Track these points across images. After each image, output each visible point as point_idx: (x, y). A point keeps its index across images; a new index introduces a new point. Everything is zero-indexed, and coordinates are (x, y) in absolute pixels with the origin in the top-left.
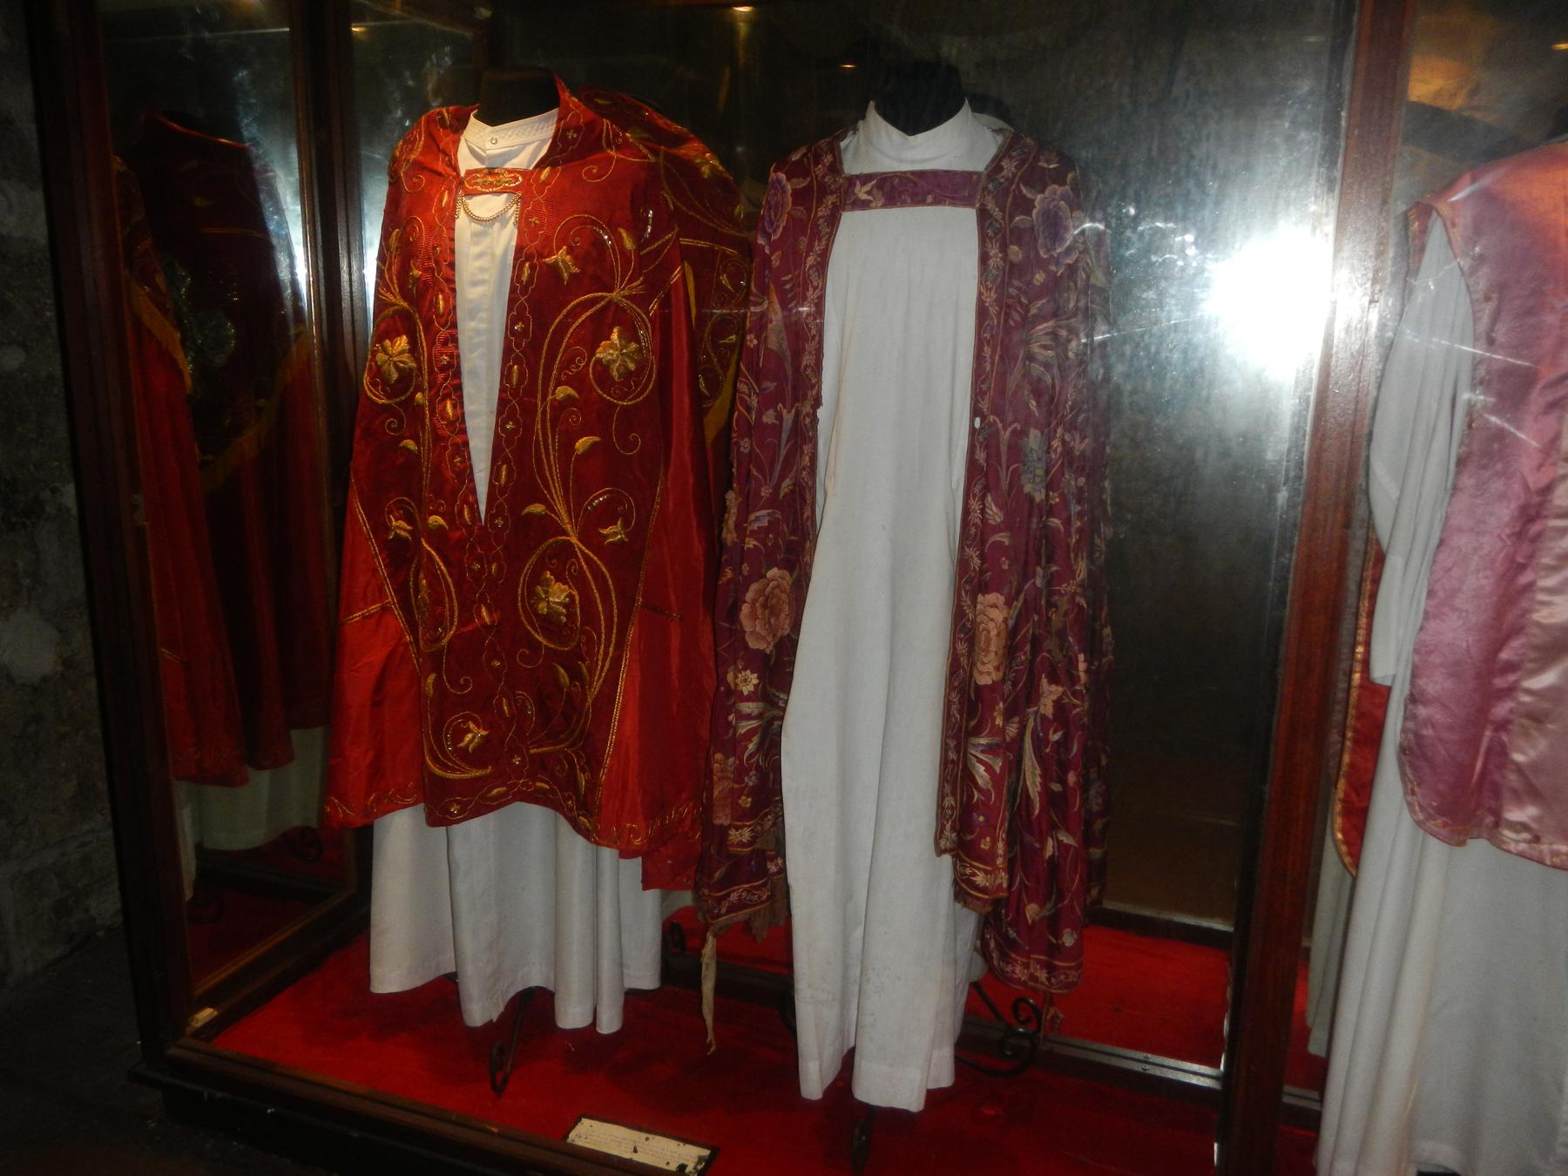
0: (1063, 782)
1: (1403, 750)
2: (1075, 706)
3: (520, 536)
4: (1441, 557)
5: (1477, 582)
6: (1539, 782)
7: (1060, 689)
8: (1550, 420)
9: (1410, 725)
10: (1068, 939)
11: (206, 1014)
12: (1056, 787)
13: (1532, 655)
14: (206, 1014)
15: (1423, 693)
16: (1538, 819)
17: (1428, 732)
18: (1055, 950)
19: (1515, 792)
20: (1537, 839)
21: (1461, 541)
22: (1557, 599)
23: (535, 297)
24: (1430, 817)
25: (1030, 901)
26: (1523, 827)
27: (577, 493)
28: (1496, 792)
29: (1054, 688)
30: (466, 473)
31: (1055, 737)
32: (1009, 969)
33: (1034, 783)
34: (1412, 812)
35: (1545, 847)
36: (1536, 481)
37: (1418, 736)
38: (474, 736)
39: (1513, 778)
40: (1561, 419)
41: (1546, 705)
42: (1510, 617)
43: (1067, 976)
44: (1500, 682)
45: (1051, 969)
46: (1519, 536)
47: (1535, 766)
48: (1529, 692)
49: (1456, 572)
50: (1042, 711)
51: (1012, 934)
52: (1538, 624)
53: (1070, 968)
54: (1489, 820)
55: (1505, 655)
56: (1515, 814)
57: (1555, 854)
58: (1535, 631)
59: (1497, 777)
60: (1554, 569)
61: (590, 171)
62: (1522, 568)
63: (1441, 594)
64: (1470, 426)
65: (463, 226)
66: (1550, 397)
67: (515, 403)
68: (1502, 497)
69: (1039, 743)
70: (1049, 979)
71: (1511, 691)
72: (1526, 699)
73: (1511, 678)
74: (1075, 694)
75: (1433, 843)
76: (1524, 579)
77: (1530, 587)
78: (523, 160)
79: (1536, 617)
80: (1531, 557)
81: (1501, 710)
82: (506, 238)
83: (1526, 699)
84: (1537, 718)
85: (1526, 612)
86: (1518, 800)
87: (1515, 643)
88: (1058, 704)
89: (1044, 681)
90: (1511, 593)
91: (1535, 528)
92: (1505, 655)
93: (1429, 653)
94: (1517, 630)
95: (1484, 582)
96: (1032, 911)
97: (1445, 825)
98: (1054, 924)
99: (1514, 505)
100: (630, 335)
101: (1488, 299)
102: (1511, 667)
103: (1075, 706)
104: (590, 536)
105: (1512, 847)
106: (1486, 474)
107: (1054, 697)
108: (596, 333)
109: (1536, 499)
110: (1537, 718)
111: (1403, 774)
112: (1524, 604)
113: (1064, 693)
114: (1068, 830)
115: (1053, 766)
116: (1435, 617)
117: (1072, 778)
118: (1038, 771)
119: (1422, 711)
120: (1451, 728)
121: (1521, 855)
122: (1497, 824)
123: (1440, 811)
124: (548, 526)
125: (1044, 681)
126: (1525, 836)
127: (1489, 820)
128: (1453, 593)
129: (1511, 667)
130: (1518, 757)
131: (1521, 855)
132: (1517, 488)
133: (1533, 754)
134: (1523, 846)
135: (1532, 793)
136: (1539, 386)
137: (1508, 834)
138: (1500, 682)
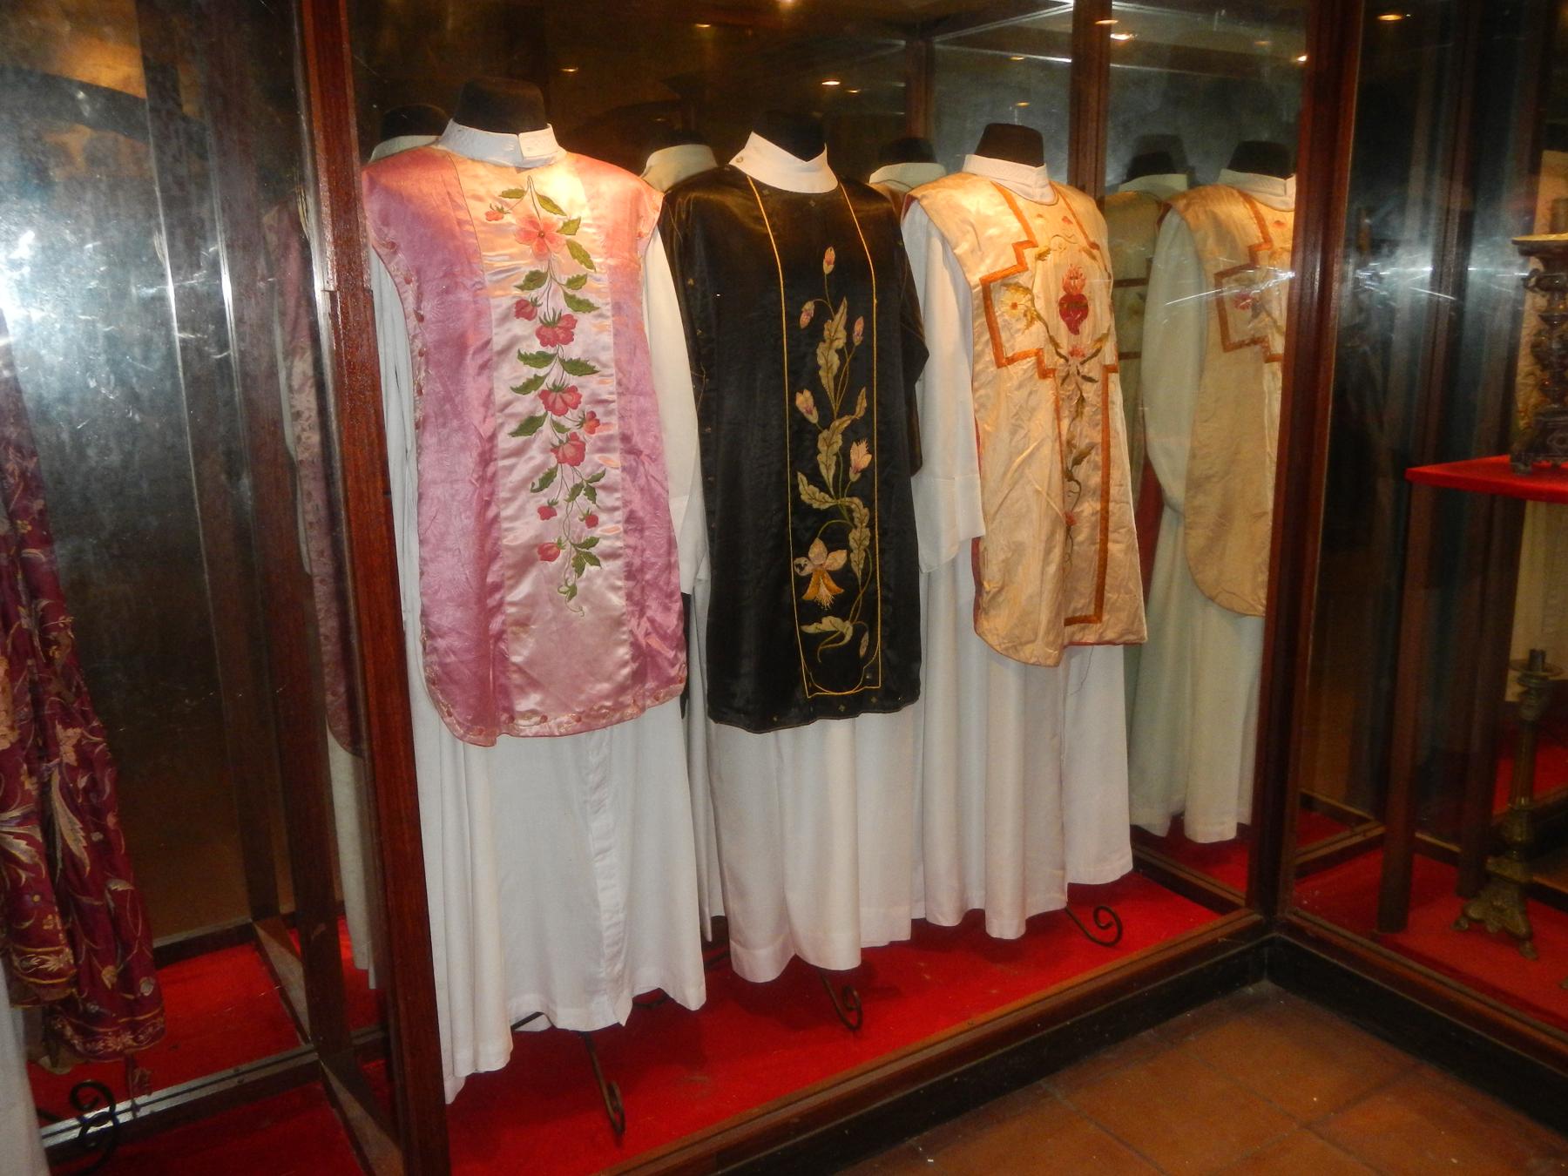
0: (102, 829)
1: (431, 681)
2: (96, 744)
4: (425, 508)
5: (463, 522)
6: (534, 674)
7: (78, 730)
8: (483, 379)
9: (434, 658)
10: (146, 989)
12: (97, 837)
13: (509, 573)
15: (438, 628)
16: (541, 703)
17: (451, 659)
18: (141, 1004)
19: (517, 686)
20: (544, 719)
21: (437, 492)
22: (517, 524)
24: (468, 730)
25: (104, 965)
26: (533, 712)
28: (505, 692)
29: (70, 732)
31: (82, 782)
32: (101, 1045)
33: (76, 840)
34: (452, 731)
35: (552, 723)
36: (486, 430)
37: (443, 665)
39: (516, 678)
40: (490, 378)
41: (527, 611)
42: (488, 547)
43: (154, 1025)
44: (491, 602)
45: (134, 1028)
46: (482, 479)
47: (531, 662)
48: (513, 604)
49: (441, 518)
50: (65, 760)
51: (93, 1008)
52: (508, 548)
53: (155, 1017)
54: (504, 717)
55: (490, 580)
56: (529, 702)
57: (559, 725)
58: (507, 553)
59: (502, 680)
60: (509, 501)
62: (488, 504)
63: (433, 540)
64: (420, 392)
66: (480, 361)
68: (463, 448)
69: (69, 795)
70: (135, 1040)
71: (501, 604)
72: (511, 610)
73: (497, 596)
74: (92, 732)
75: (474, 749)
76: (491, 513)
77: (496, 519)
79: (505, 542)
80: (492, 494)
81: (495, 625)
83: (511, 610)
84: (523, 623)
85: (498, 539)
86: (522, 691)
87: (496, 567)
88: (78, 748)
89: (59, 727)
90: (487, 527)
91: (490, 470)
92: (490, 580)
93: (436, 592)
94: (494, 556)
95: (466, 522)
96: (108, 975)
97: (481, 732)
98: (127, 980)
99: (475, 454)
101: (408, 282)
102: (497, 587)
103: (96, 744)
105: (528, 732)
106: (445, 432)
107: (74, 741)
109: (487, 447)
110: (523, 623)
111: (436, 703)
112: (495, 534)
113: (83, 736)
114: (119, 877)
115: (89, 815)
116: (432, 561)
117: (111, 820)
118: (78, 825)
119: (441, 643)
120: (468, 650)
121: (536, 736)
122: (512, 719)
123: (474, 722)
125: (59, 727)
126: (536, 719)
127: (504, 717)
128: (443, 536)
129: (497, 587)
130: (516, 659)
131: (536, 736)
132: (475, 440)
133: (526, 653)
134: (536, 729)
135: (534, 684)
136: (471, 351)
137: (521, 722)
138: (491, 602)
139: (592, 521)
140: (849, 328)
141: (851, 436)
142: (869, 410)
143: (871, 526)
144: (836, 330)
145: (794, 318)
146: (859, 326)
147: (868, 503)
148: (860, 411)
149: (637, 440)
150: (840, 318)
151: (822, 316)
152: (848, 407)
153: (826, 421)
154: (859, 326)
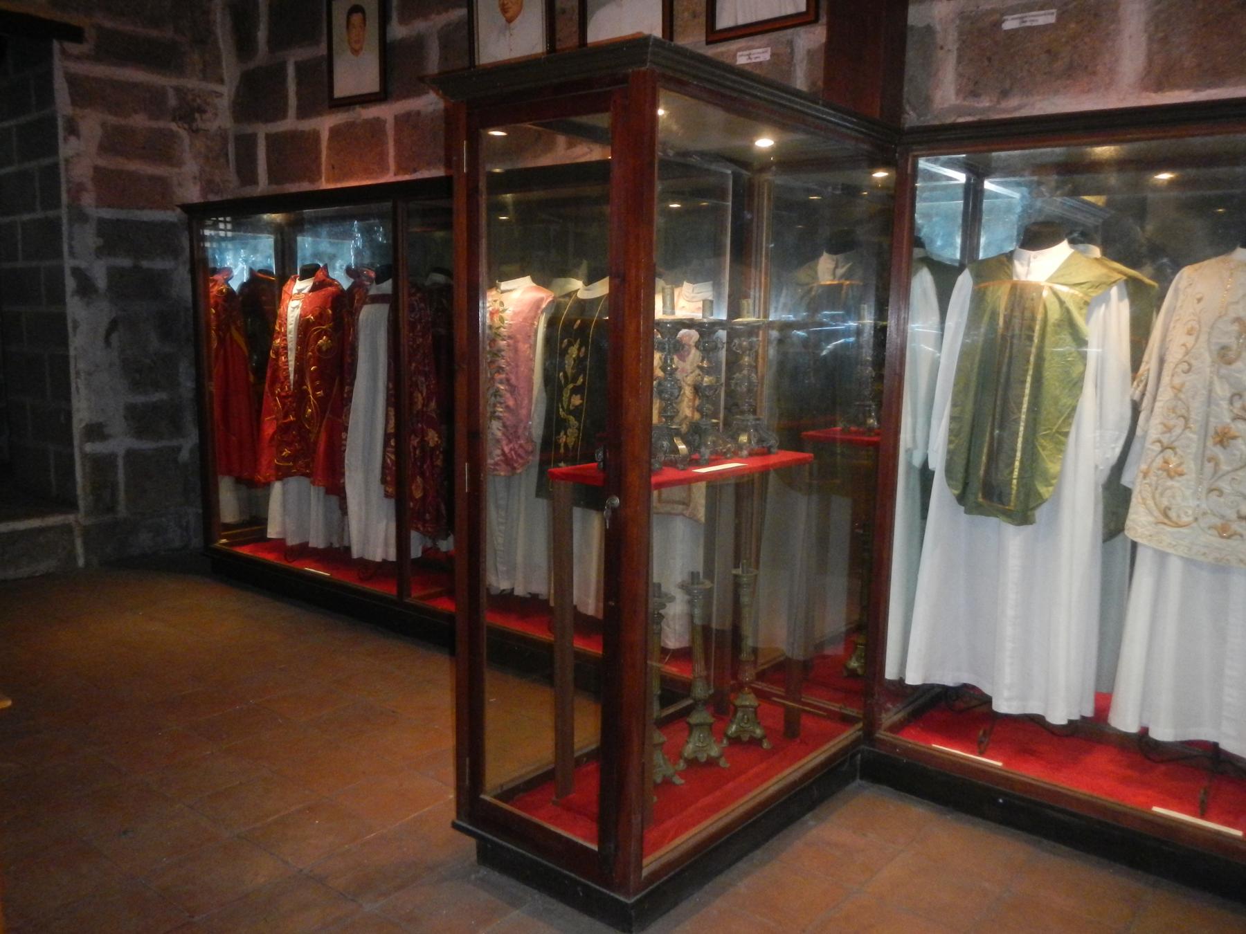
3: (300, 395)
11: (224, 541)
14: (224, 541)
23: (304, 326)
27: (312, 382)
30: (287, 377)
38: (286, 452)
61: (322, 293)
65: (290, 309)
67: (298, 358)
78: (306, 291)
82: (297, 312)
100: (329, 337)
104: (314, 395)
108: (319, 337)
124: (306, 392)
139: (495, 406)
140: (579, 350)
141: (575, 391)
142: (584, 383)
143: (579, 429)
144: (573, 351)
145: (561, 343)
146: (583, 349)
147: (578, 418)
148: (581, 380)
149: (513, 381)
150: (576, 346)
151: (570, 344)
152: (575, 379)
153: (567, 383)
154: (583, 349)
